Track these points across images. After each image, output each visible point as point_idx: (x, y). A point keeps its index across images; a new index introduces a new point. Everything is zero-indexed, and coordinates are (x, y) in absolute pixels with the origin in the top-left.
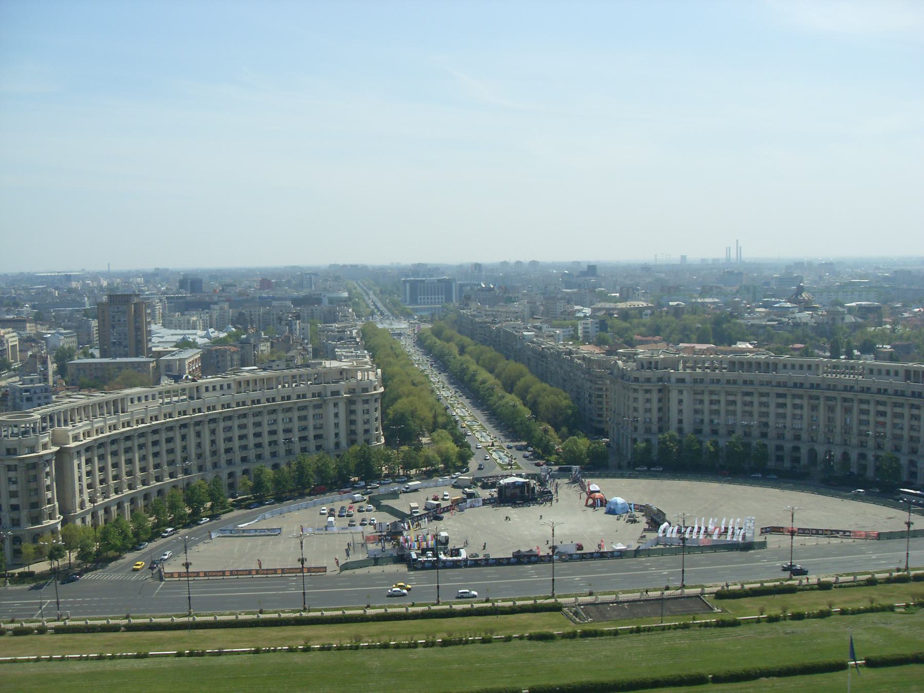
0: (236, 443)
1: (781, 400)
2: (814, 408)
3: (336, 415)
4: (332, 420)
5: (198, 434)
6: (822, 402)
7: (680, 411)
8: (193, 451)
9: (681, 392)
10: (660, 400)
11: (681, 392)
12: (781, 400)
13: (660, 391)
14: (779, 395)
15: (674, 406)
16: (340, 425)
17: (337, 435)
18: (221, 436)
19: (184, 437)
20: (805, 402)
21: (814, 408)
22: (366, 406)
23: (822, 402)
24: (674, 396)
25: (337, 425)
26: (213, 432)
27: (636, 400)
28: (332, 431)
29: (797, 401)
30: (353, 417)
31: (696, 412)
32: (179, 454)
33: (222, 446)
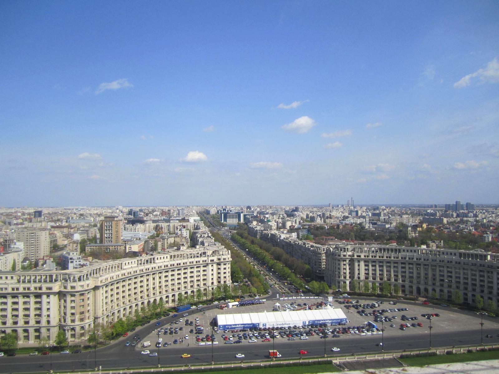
0: (170, 283)
1: (403, 265)
3: (212, 270)
4: (211, 272)
7: (359, 269)
8: (151, 286)
12: (403, 265)
14: (402, 263)
17: (212, 279)
18: (163, 279)
19: (148, 280)
22: (225, 266)
25: (212, 274)
26: (160, 278)
27: (339, 264)
30: (219, 271)
33: (163, 284)
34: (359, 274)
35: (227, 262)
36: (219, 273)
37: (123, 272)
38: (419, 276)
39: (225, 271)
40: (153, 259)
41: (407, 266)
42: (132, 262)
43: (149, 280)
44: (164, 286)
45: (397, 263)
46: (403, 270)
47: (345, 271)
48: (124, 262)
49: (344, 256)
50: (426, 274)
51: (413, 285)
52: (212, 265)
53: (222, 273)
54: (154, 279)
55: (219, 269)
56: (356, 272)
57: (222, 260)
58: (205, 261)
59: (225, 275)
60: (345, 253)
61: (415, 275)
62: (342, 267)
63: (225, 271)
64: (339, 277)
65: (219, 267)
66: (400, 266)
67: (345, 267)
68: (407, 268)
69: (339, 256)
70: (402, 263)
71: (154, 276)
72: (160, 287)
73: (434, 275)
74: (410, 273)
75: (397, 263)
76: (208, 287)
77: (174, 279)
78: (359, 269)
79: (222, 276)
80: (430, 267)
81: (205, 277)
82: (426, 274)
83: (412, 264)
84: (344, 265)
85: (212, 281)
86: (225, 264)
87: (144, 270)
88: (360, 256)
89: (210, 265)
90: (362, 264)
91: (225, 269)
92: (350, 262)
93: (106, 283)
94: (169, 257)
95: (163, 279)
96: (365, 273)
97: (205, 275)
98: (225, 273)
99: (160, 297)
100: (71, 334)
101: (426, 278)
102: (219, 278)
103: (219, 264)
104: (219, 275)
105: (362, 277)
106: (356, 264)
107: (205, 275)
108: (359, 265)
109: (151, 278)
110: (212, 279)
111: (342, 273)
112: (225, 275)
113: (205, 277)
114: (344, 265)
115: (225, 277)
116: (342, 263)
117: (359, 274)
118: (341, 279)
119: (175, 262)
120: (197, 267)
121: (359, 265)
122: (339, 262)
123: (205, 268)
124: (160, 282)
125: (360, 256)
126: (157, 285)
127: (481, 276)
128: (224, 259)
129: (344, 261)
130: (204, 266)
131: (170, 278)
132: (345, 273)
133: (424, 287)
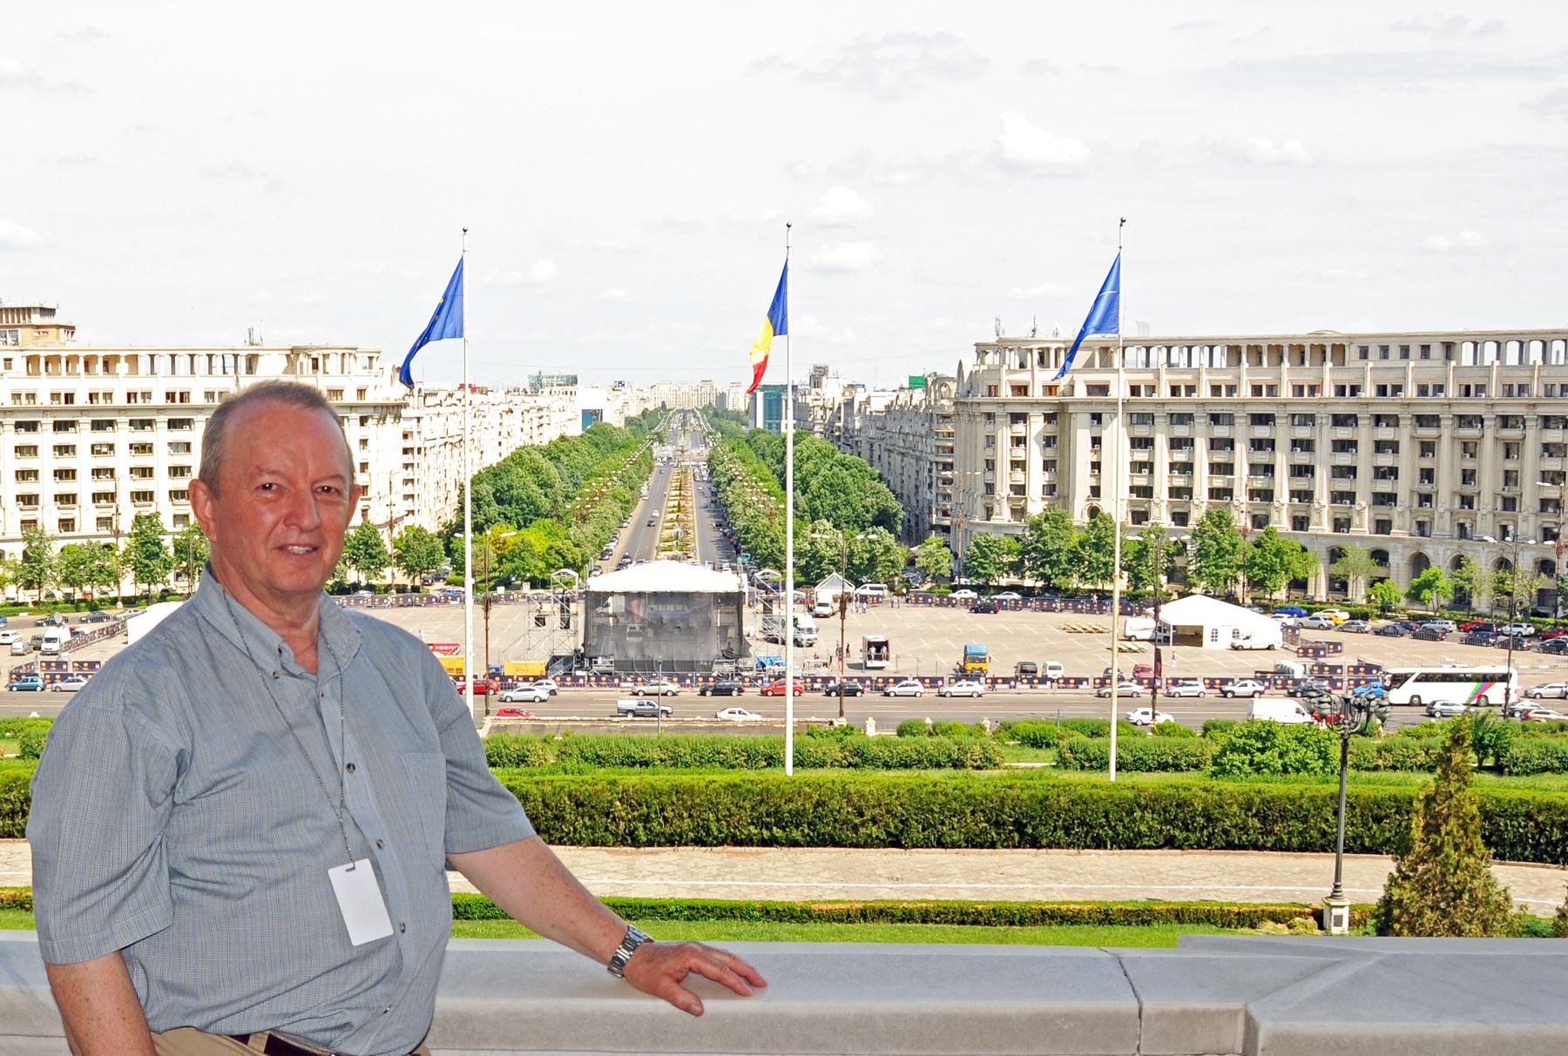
1: (1344, 433)
2: (1427, 448)
6: (1446, 431)
7: (1096, 466)
9: (1097, 417)
10: (1049, 441)
11: (1097, 417)
12: (1344, 433)
13: (1049, 418)
14: (1339, 421)
15: (1083, 454)
20: (1404, 434)
21: (1427, 448)
23: (1446, 431)
27: (991, 441)
29: (1385, 433)
31: (1138, 467)
34: (1096, 491)
38: (1426, 488)
46: (1344, 459)
47: (1019, 476)
49: (1021, 389)
50: (1468, 476)
56: (1083, 481)
60: (1022, 378)
61: (1405, 486)
62: (1005, 452)
64: (989, 512)
66: (1325, 435)
67: (1019, 453)
69: (993, 390)
70: (1339, 421)
73: (1510, 478)
78: (1096, 466)
80: (1490, 432)
82: (1468, 476)
83: (1393, 421)
84: (1019, 441)
88: (1103, 389)
90: (1116, 434)
96: (1132, 489)
101: (1467, 501)
105: (1117, 505)
106: (1083, 437)
108: (1096, 441)
111: (1003, 490)
114: (1019, 441)
116: (1005, 434)
117: (1096, 491)
121: (1096, 441)
122: (989, 429)
125: (1103, 389)
129: (1018, 418)
132: (1020, 490)
133: (1450, 555)
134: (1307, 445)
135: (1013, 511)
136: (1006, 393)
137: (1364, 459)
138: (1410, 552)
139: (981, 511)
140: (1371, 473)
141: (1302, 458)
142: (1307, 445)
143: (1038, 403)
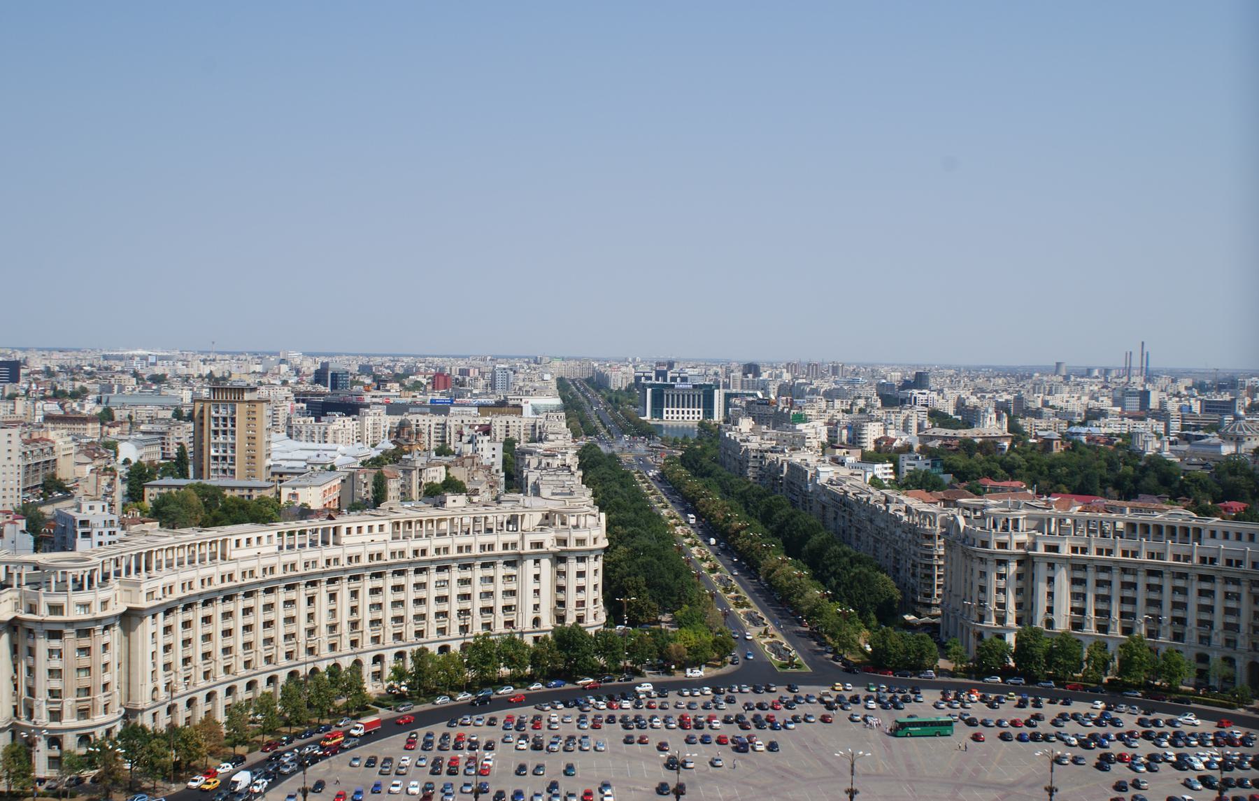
0: (388, 613)
1: (1206, 586)
3: (537, 577)
4: (531, 585)
5: (333, 596)
7: (1051, 594)
8: (323, 620)
11: (1051, 566)
12: (1206, 586)
13: (1020, 563)
14: (1203, 578)
16: (542, 592)
17: (536, 607)
18: (366, 599)
19: (311, 600)
22: (582, 567)
24: (1042, 571)
25: (537, 591)
26: (354, 594)
27: (983, 574)
28: (530, 600)
30: (562, 582)
32: (303, 624)
33: (366, 615)
35: (591, 551)
36: (561, 589)
37: (226, 568)
39: (581, 581)
40: (335, 533)
41: (1219, 588)
42: (259, 538)
43: (317, 599)
44: (367, 623)
45: (1106, 569)
46: (1205, 601)
47: (1002, 598)
48: (234, 538)
49: (1003, 545)
51: (1236, 656)
52: (537, 561)
53: (572, 590)
54: (333, 596)
55: (562, 574)
57: (572, 545)
58: (514, 545)
59: (581, 596)
60: (1005, 538)
62: (993, 582)
63: (581, 581)
65: (562, 567)
66: (1194, 587)
68: (1219, 595)
69: (985, 544)
70: (1203, 578)
71: (332, 588)
72: (354, 625)
74: (1176, 605)
75: (1106, 569)
76: (522, 633)
77: (401, 603)
78: (1051, 594)
79: (572, 597)
81: (512, 601)
83: (1237, 582)
85: (535, 615)
86: (581, 559)
87: (298, 567)
88: (1055, 549)
89: (530, 562)
91: (581, 574)
92: (1021, 568)
93: (164, 601)
94: (388, 527)
95: (366, 599)
96: (1072, 609)
97: (512, 593)
98: (580, 589)
99: (353, 658)
100: (50, 758)
102: (561, 603)
103: (559, 559)
104: (561, 597)
107: (512, 593)
108: (1051, 580)
109: (322, 592)
110: (536, 607)
112: (581, 596)
113: (512, 601)
114: (1001, 576)
115: (581, 604)
118: (986, 624)
119: (409, 546)
120: (484, 566)
122: (983, 568)
123: (510, 571)
124: (354, 610)
125: (1055, 549)
126: (344, 617)
127: (1125, 585)
128: (581, 541)
130: (507, 563)
131: (388, 597)
132: (1002, 606)
134: (1183, 591)
135: (997, 618)
136: (993, 547)
137: (1219, 603)
138: (1248, 661)
139: (976, 617)
140: (1222, 610)
141: (1179, 598)
142: (1183, 591)
143: (1014, 554)
